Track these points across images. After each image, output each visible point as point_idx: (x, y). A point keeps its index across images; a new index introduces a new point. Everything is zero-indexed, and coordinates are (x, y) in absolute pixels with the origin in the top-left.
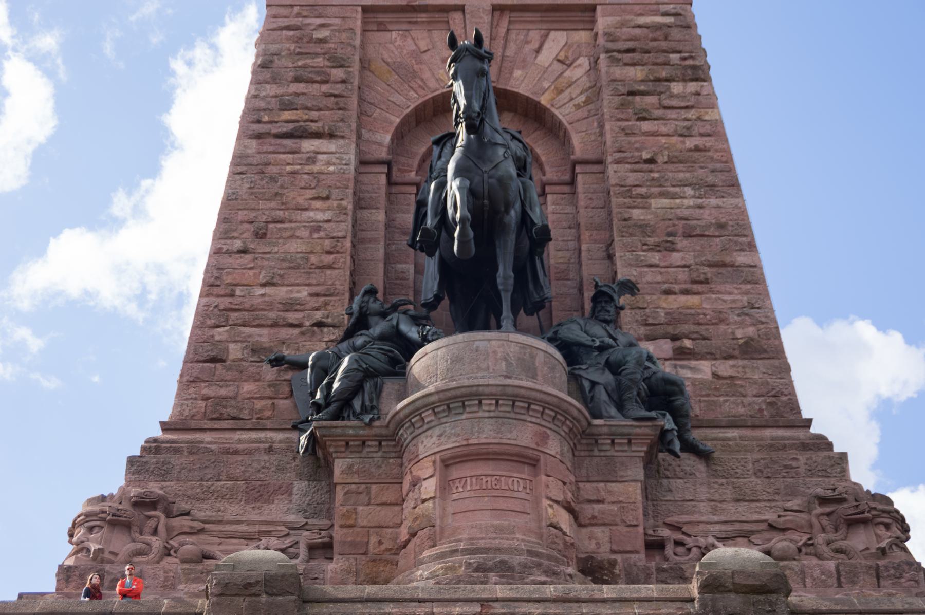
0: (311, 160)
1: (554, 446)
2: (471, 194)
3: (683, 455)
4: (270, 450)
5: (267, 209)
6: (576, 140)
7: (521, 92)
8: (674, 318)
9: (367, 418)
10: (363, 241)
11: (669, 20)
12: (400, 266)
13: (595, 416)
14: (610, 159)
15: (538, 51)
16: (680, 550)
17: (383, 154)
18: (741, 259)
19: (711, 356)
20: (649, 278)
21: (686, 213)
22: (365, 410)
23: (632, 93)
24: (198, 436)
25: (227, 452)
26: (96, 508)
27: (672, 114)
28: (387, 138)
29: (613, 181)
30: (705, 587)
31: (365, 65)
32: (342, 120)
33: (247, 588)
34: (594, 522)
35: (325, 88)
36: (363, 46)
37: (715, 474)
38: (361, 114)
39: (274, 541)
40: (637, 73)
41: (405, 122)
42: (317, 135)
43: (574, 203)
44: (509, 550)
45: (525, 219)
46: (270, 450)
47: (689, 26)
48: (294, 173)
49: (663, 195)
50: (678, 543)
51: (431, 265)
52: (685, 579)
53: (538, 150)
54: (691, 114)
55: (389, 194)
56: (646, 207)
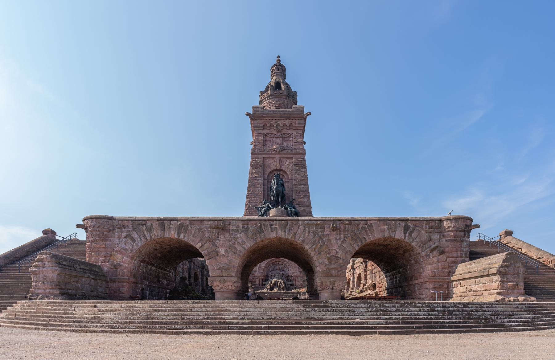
0: (258, 181)
2: (276, 192)
5: (253, 188)
6: (289, 177)
7: (283, 169)
8: (299, 202)
11: (302, 159)
15: (285, 163)
17: (266, 179)
18: (308, 195)
19: (303, 207)
20: (297, 197)
21: (302, 188)
28: (267, 176)
29: (293, 184)
31: (264, 165)
35: (259, 170)
36: (264, 163)
38: (264, 172)
40: (297, 168)
43: (289, 184)
45: (283, 193)
47: (304, 160)
49: (299, 186)
53: (285, 177)
54: (303, 174)
56: (297, 187)
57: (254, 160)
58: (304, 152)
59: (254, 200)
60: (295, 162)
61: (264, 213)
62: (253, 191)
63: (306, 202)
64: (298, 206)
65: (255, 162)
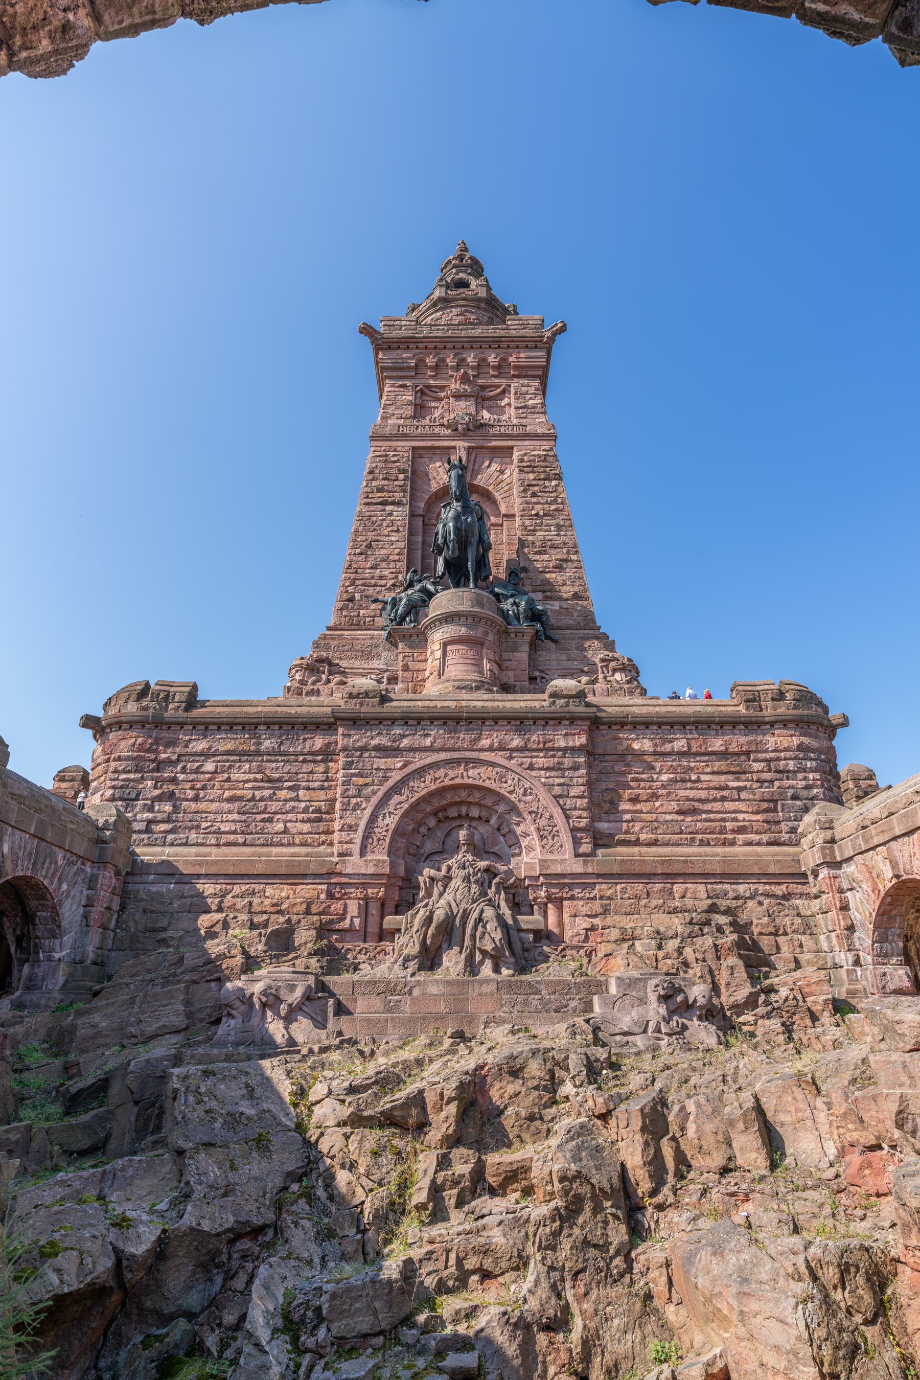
0: (391, 514)
1: (491, 637)
2: (456, 528)
3: (546, 641)
4: (372, 638)
9: (412, 625)
10: (412, 549)
12: (428, 561)
13: (509, 624)
14: (517, 514)
16: (544, 680)
17: (421, 512)
18: (574, 557)
22: (411, 622)
23: (528, 485)
24: (342, 632)
25: (354, 639)
26: (299, 662)
27: (544, 494)
30: (551, 696)
32: (404, 496)
33: (358, 696)
34: (507, 669)
35: (396, 483)
37: (560, 649)
39: (373, 676)
40: (531, 476)
41: (430, 498)
42: (393, 503)
44: (472, 681)
45: (481, 541)
46: (372, 638)
48: (383, 520)
49: (541, 530)
50: (542, 678)
51: (441, 560)
52: (544, 692)
53: (488, 511)
55: (424, 529)
57: (379, 454)
58: (552, 431)
59: (373, 578)
60: (522, 461)
61: (407, 613)
62: (369, 546)
63: (568, 583)
64: (540, 595)
65: (386, 461)
